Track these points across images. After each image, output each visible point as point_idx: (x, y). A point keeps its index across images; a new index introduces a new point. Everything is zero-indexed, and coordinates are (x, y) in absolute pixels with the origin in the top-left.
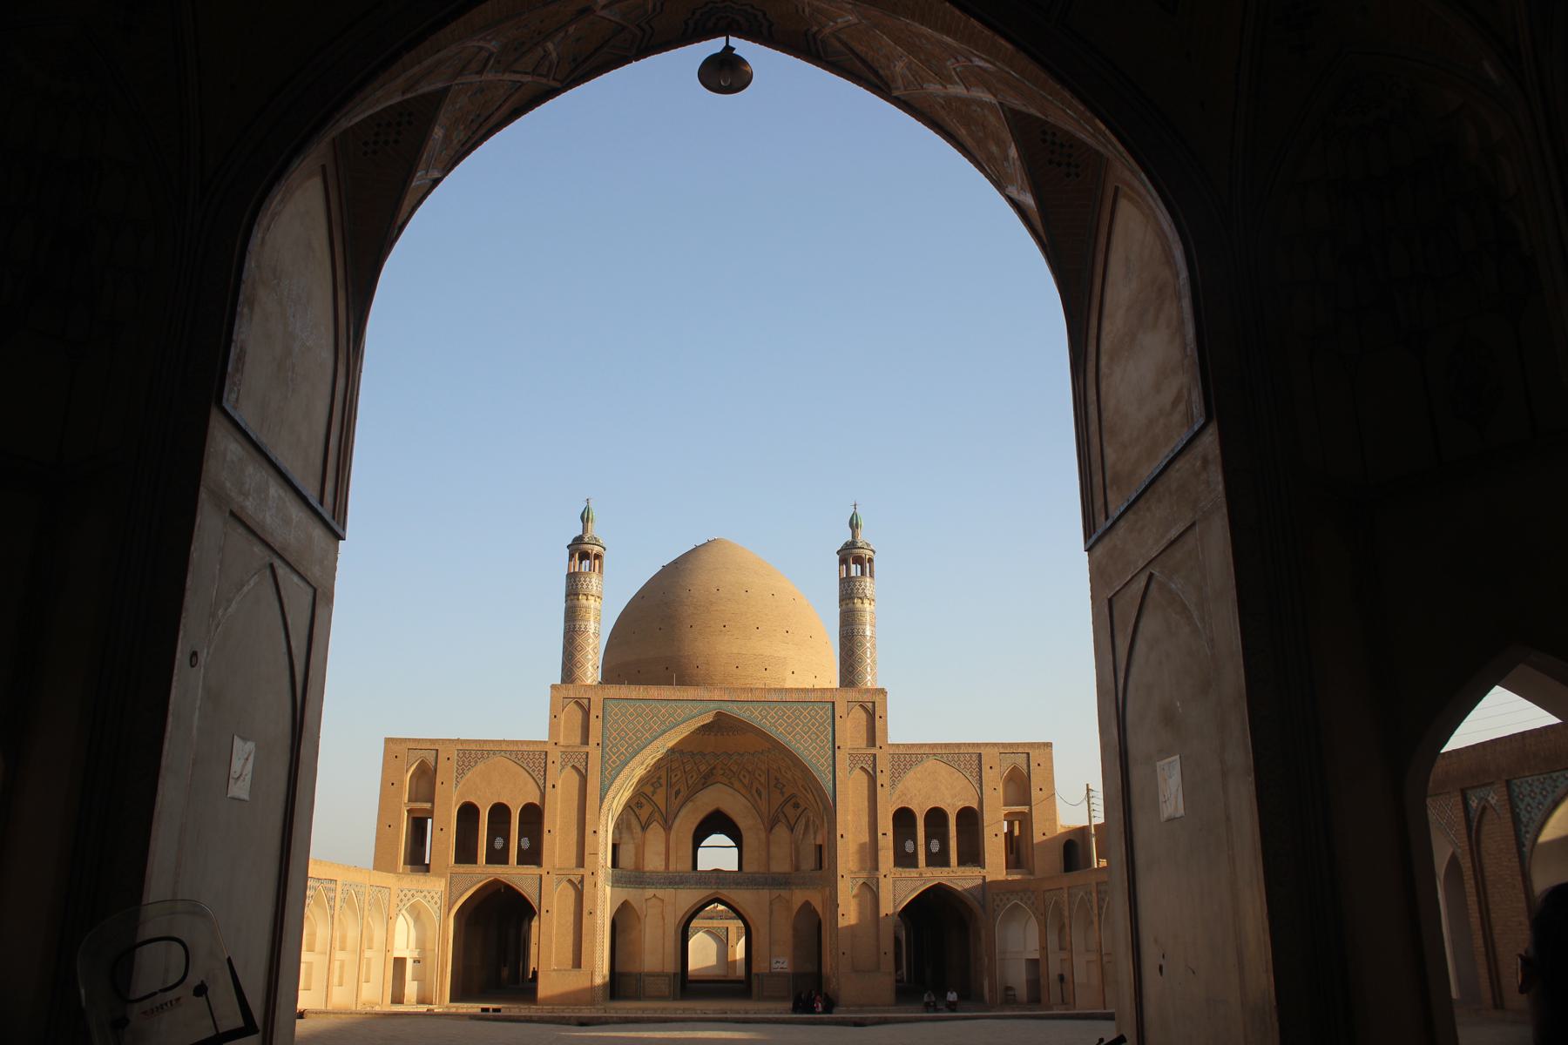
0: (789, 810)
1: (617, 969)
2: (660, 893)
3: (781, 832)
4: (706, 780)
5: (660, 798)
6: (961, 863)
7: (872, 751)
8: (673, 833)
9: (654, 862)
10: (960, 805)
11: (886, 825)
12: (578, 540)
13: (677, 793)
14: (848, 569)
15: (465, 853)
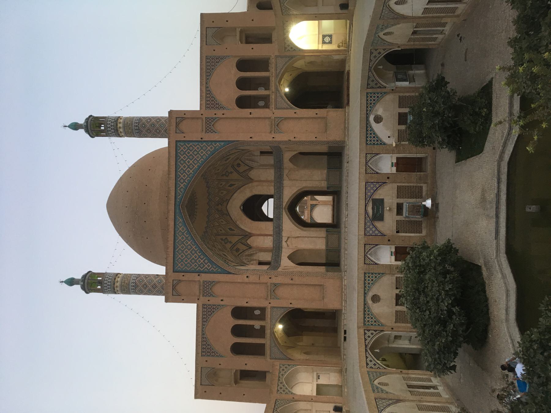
0: (242, 169)
1: (324, 261)
2: (284, 239)
3: (253, 174)
4: (225, 214)
5: (235, 239)
6: (267, 70)
7: (204, 119)
8: (254, 232)
9: (268, 242)
10: (234, 69)
11: (246, 112)
12: (83, 288)
13: (230, 229)
14: (102, 131)
15: (257, 350)
